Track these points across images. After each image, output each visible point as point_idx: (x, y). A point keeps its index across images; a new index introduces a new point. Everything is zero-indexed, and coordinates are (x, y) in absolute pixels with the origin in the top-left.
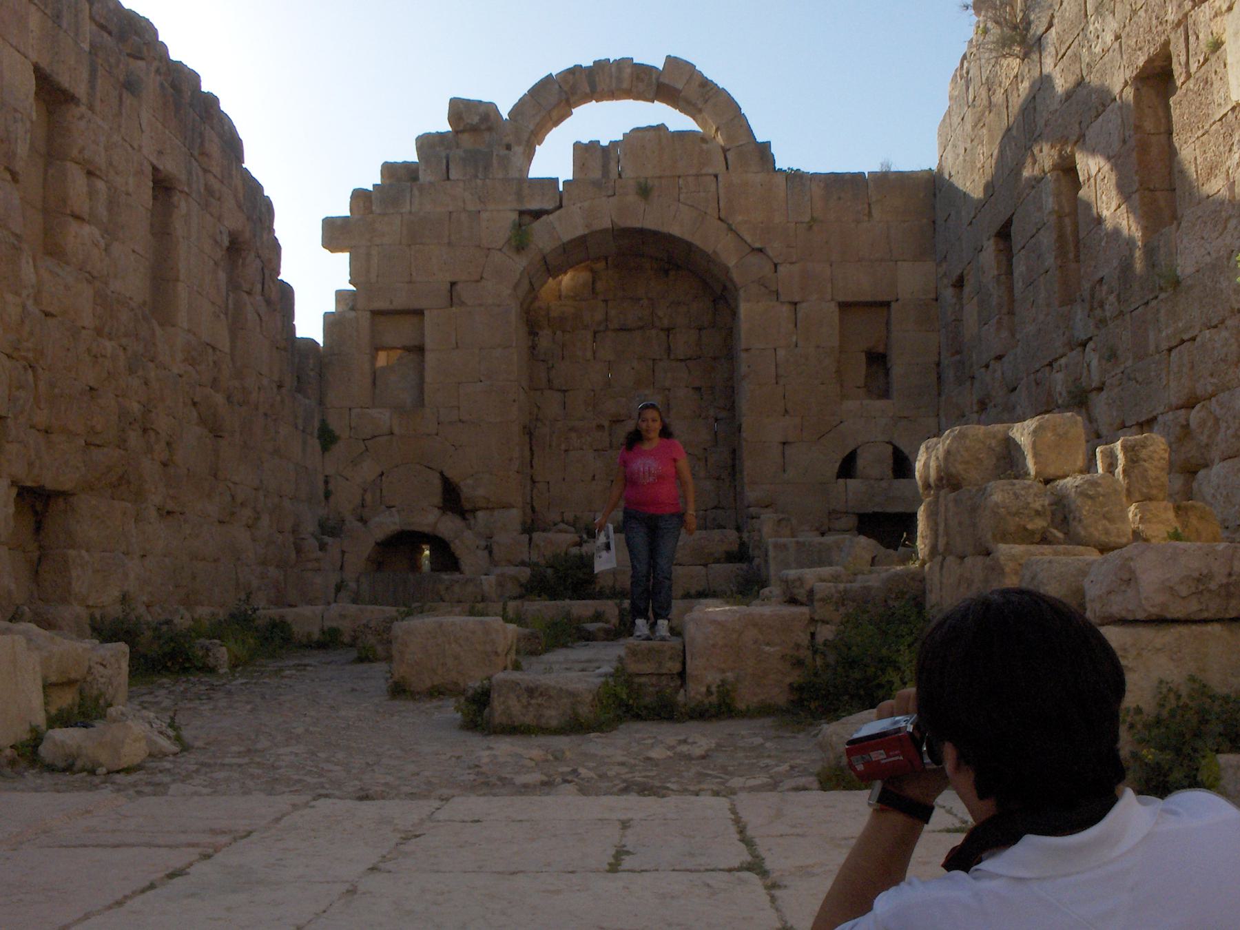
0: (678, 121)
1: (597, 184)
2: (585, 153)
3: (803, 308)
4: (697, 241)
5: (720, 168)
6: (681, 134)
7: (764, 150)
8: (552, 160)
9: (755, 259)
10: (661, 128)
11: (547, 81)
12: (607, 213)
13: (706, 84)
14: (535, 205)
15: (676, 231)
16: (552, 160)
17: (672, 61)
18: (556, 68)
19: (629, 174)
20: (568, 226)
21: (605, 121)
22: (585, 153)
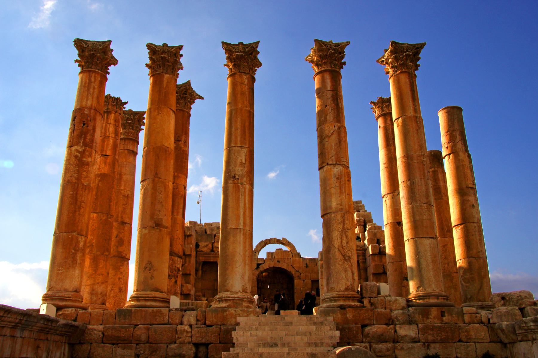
0: (285, 248)
1: (271, 259)
2: (269, 254)
3: (305, 281)
4: (287, 269)
5: (291, 256)
6: (285, 251)
7: (299, 255)
8: (262, 255)
9: (297, 273)
10: (281, 249)
11: (262, 242)
12: (272, 264)
13: (289, 242)
14: (260, 263)
15: (284, 267)
16: (262, 255)
17: (283, 239)
18: (264, 239)
19: (276, 257)
20: (265, 266)
21: (272, 248)
22: (269, 254)
